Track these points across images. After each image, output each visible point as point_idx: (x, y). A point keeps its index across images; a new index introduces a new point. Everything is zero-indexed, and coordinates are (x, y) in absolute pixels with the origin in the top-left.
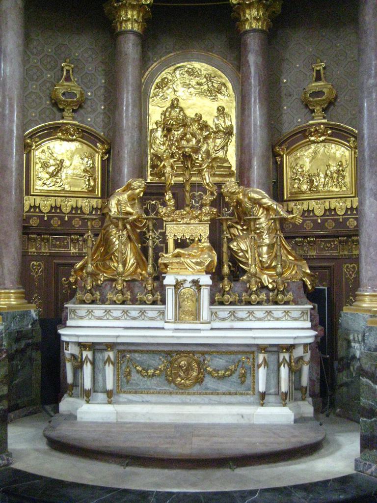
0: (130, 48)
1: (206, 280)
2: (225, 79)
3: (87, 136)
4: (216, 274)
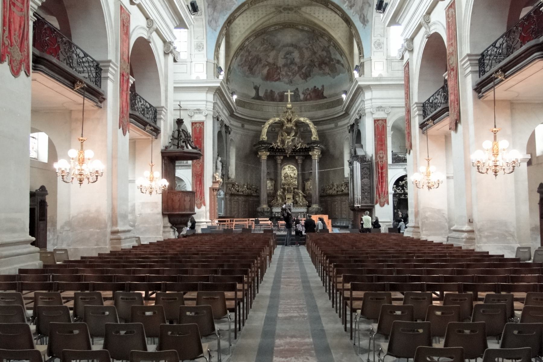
0: (279, 166)
3: (271, 179)
4: (294, 203)
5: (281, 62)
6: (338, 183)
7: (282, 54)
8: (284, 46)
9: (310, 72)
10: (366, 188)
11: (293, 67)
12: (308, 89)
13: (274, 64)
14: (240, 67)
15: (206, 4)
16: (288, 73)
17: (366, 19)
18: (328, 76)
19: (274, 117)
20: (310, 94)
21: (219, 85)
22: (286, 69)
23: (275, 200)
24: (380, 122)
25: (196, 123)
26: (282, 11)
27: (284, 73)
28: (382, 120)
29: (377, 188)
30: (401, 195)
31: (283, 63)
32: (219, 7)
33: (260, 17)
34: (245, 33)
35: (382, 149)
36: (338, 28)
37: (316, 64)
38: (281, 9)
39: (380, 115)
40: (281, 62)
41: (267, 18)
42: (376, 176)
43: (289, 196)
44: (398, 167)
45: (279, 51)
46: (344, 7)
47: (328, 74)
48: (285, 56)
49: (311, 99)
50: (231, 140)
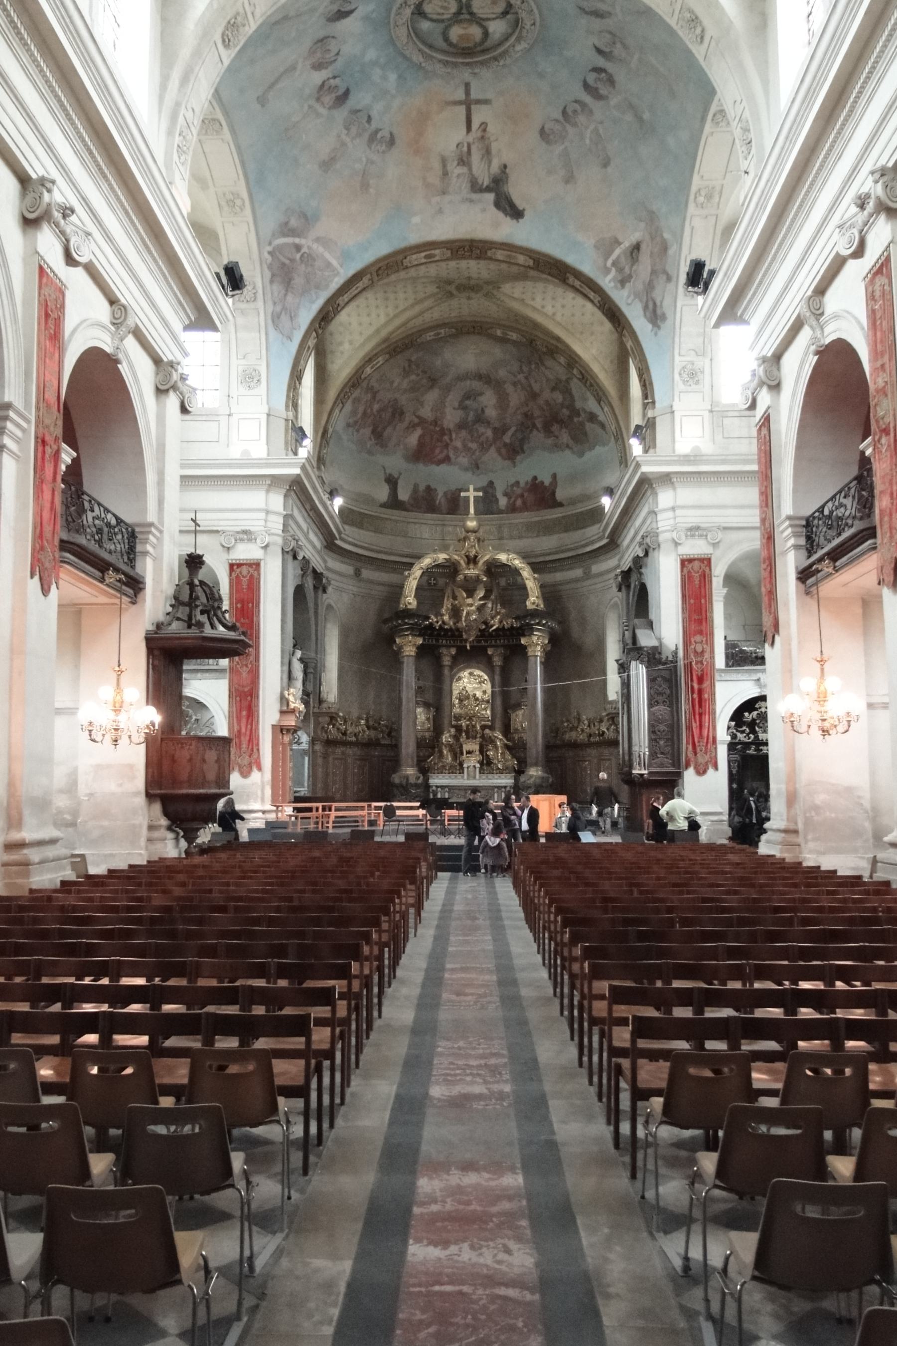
0: (446, 671)
1: (478, 765)
2: (486, 677)
3: (427, 705)
4: (481, 763)
5: (451, 417)
6: (591, 715)
7: (453, 399)
8: (460, 378)
9: (522, 441)
10: (662, 727)
11: (482, 429)
12: (518, 483)
13: (435, 422)
14: (351, 429)
15: (268, 274)
16: (470, 445)
17: (659, 312)
18: (568, 452)
19: (435, 551)
20: (522, 496)
21: (297, 471)
22: (464, 433)
23: (437, 755)
24: (696, 564)
25: (239, 565)
26: (455, 292)
27: (459, 444)
28: (702, 560)
29: (689, 728)
30: (747, 745)
31: (457, 420)
32: (298, 281)
33: (401, 308)
34: (363, 345)
35: (701, 632)
36: (592, 334)
37: (539, 425)
38: (452, 288)
39: (696, 548)
40: (451, 417)
41: (417, 309)
42: (687, 699)
43: (472, 746)
44: (740, 676)
45: (448, 389)
46: (607, 282)
47: (568, 446)
48: (461, 402)
49: (525, 508)
50: (329, 607)
